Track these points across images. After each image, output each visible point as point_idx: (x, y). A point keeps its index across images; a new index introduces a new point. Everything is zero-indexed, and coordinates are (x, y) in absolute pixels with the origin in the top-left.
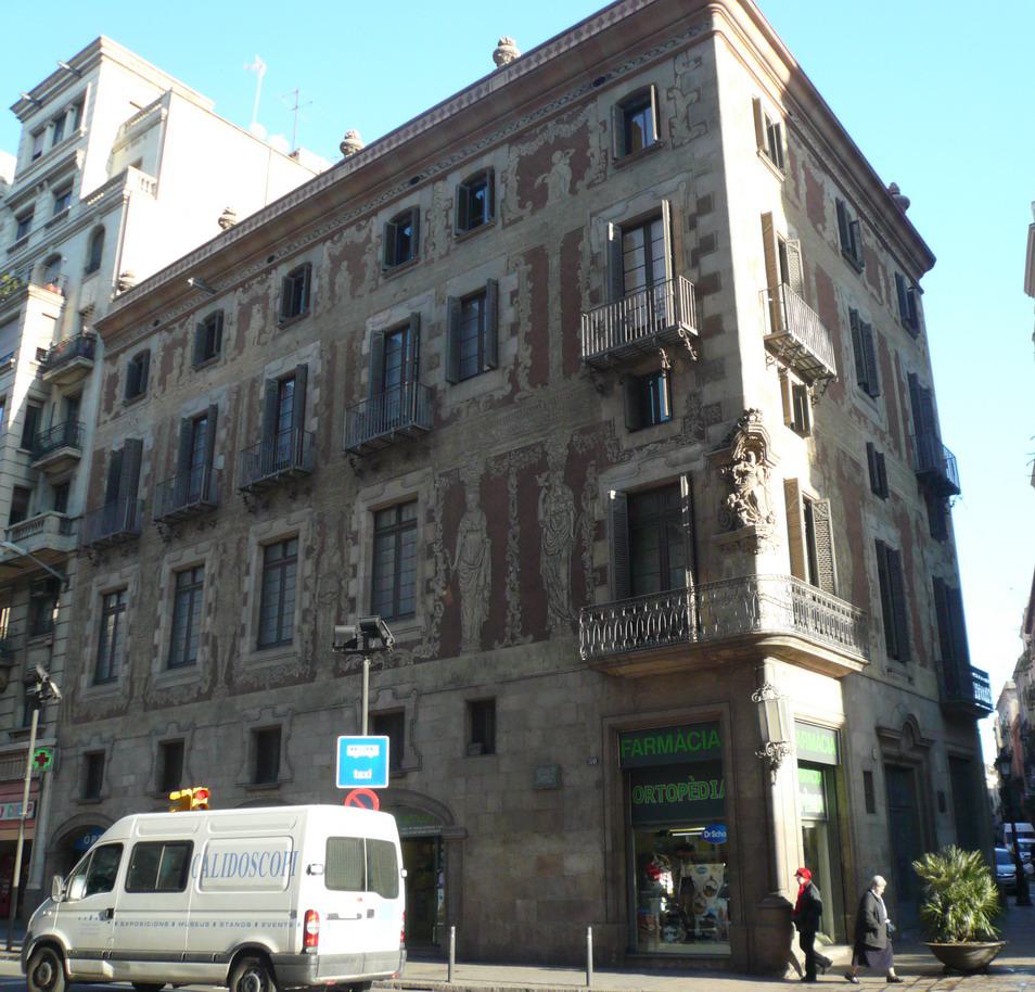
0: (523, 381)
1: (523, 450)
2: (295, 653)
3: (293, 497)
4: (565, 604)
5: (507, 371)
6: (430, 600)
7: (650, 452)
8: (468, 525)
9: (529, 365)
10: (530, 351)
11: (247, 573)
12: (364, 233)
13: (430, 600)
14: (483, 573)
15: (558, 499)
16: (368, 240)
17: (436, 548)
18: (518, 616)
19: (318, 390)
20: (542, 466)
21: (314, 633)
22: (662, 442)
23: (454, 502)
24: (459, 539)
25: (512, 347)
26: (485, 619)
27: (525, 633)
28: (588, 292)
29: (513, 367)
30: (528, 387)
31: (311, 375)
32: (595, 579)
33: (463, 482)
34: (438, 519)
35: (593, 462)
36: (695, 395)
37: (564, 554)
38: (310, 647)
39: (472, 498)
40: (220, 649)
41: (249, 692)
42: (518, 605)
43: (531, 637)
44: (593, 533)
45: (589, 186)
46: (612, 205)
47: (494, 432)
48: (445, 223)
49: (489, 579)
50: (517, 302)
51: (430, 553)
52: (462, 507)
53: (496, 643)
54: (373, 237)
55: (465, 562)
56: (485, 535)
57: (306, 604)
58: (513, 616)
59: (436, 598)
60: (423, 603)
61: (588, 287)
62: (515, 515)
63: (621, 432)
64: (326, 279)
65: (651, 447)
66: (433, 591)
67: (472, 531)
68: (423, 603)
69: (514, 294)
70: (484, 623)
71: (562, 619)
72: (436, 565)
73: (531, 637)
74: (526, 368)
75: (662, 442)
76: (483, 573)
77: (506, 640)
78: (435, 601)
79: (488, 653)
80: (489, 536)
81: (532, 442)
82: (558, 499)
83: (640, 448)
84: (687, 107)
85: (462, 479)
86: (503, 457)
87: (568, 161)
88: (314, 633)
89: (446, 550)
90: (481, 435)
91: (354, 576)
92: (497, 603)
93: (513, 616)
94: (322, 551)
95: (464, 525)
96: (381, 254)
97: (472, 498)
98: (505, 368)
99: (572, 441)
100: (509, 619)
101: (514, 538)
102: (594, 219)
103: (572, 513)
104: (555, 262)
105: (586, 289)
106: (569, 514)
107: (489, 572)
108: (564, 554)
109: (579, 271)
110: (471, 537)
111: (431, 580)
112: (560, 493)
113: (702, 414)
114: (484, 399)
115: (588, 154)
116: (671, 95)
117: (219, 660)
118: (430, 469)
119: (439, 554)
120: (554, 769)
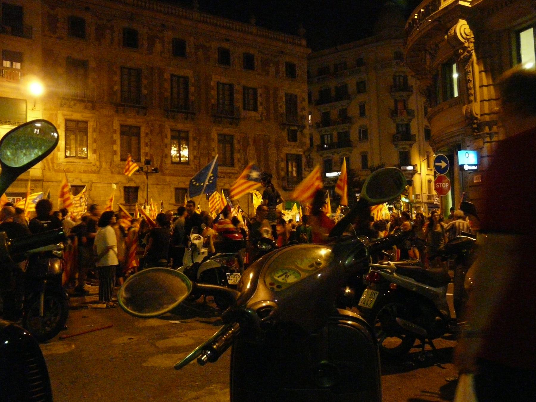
2: (192, 168)
3: (186, 119)
6: (240, 164)
17: (241, 151)
19: (193, 88)
20: (269, 141)
24: (248, 151)
25: (260, 108)
38: (198, 167)
39: (251, 142)
51: (239, 152)
57: (195, 154)
91: (214, 150)
97: (251, 142)
110: (251, 151)
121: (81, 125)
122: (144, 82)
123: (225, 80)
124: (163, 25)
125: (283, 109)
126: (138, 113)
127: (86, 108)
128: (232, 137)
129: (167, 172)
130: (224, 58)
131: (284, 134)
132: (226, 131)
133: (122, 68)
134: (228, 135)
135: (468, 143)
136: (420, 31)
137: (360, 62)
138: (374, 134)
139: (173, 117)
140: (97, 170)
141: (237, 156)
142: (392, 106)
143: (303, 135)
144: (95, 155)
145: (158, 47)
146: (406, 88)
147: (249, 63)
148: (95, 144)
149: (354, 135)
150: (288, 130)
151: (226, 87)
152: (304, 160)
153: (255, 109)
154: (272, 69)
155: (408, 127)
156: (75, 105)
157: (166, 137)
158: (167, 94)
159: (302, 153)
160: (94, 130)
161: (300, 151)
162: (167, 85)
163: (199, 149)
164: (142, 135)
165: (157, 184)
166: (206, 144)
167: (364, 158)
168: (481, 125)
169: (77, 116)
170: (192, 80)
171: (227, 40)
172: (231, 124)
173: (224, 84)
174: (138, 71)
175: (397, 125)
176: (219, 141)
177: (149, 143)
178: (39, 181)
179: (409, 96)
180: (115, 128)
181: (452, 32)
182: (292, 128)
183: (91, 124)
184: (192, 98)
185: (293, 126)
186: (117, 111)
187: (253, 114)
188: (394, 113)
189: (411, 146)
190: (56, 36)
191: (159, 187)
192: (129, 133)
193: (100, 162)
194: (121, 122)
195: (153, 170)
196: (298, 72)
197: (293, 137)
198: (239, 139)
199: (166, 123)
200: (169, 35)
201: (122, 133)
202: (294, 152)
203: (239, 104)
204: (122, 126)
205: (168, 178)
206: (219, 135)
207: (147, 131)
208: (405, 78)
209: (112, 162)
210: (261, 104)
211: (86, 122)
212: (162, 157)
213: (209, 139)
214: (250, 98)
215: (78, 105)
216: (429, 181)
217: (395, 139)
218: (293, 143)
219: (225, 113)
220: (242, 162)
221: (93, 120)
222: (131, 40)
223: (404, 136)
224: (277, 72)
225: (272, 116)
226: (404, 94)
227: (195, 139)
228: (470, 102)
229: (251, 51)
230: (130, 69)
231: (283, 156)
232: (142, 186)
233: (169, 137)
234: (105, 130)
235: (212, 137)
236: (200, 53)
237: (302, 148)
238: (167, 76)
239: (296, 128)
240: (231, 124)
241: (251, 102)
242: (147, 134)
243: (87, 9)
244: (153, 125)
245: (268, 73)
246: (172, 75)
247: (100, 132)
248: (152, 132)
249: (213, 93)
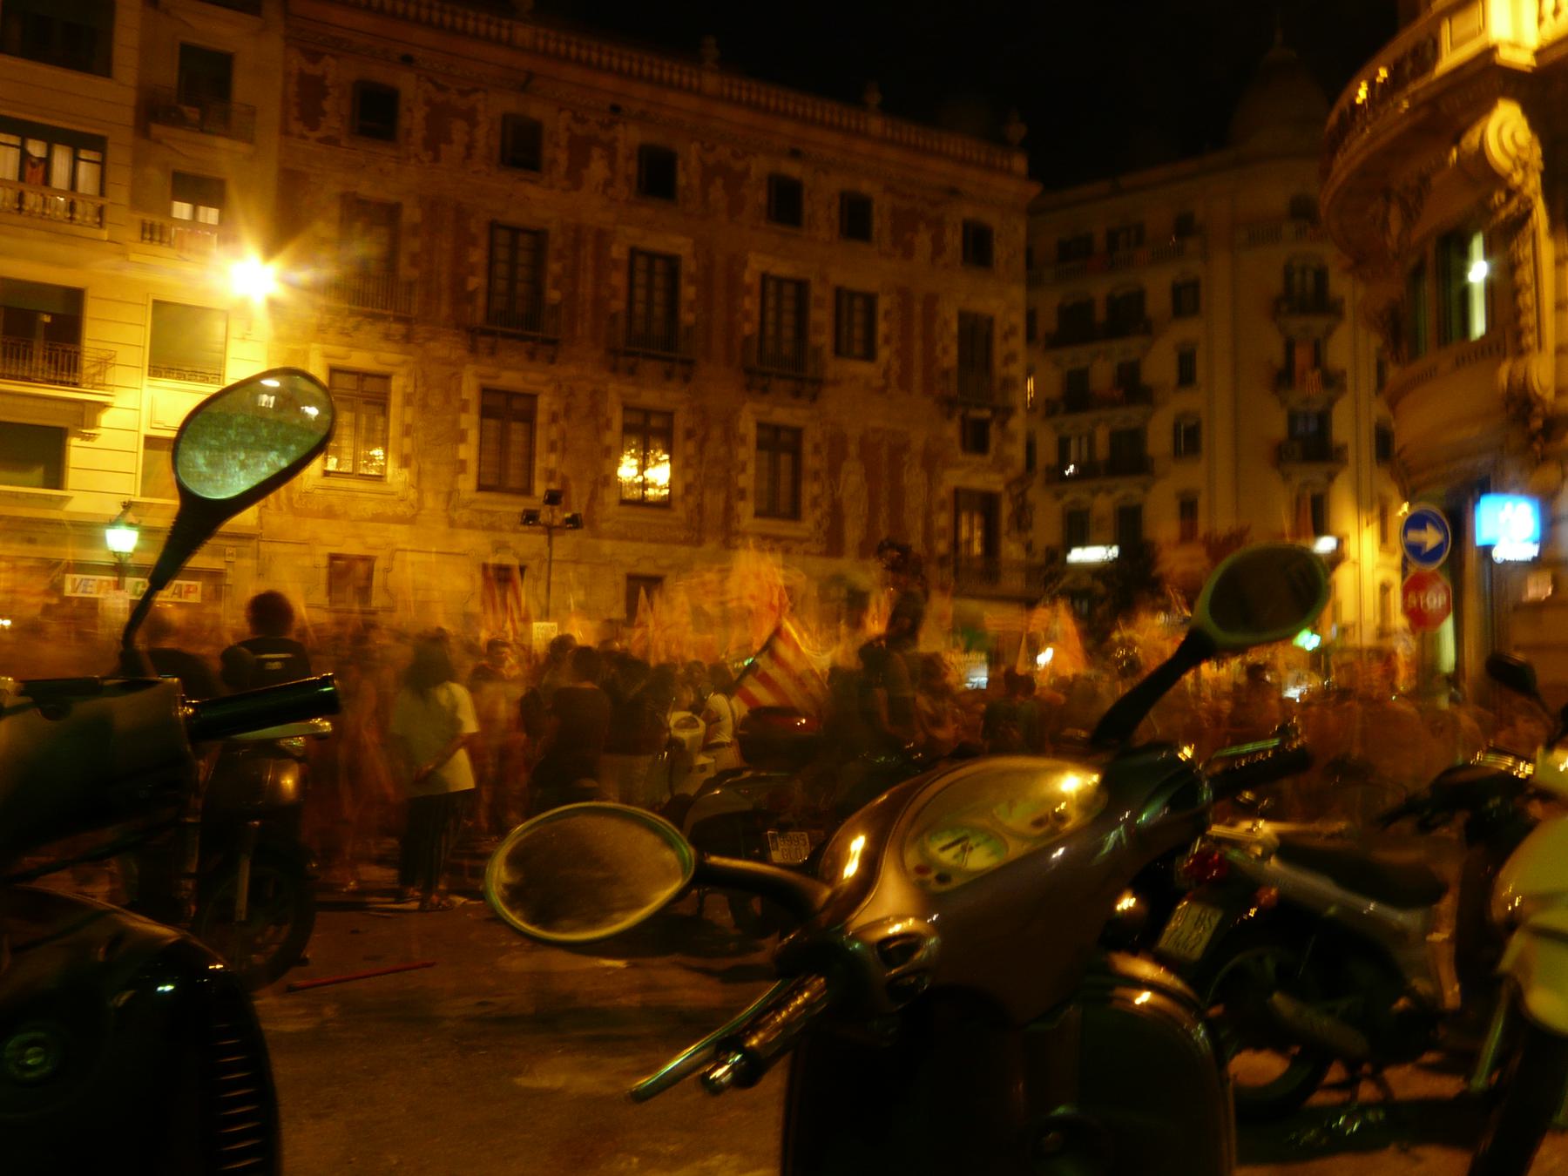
3: (669, 376)
21: (700, 507)
23: (836, 447)
24: (843, 476)
25: (884, 353)
39: (853, 449)
51: (816, 476)
69: (887, 313)
88: (700, 507)
91: (743, 470)
94: (705, 439)
97: (853, 449)
104: (918, 308)
121: (371, 385)
122: (554, 267)
123: (783, 269)
124: (615, 109)
125: (949, 358)
126: (532, 356)
127: (387, 337)
128: (797, 433)
129: (605, 526)
130: (786, 203)
131: (952, 430)
132: (782, 415)
133: (494, 226)
134: (787, 428)
135: (1512, 475)
136: (1372, 139)
137: (1185, 227)
138: (1218, 437)
139: (632, 371)
140: (410, 512)
141: (810, 489)
142: (1279, 359)
143: (1009, 437)
144: (405, 472)
145: (597, 169)
146: (1320, 303)
147: (855, 219)
148: (407, 441)
149: (1159, 439)
150: (963, 418)
151: (789, 290)
152: (1006, 509)
153: (869, 355)
154: (923, 240)
155: (1324, 420)
156: (356, 328)
157: (608, 425)
158: (618, 305)
159: (1000, 488)
160: (408, 400)
162: (618, 279)
163: (701, 462)
164: (541, 418)
165: (577, 562)
166: (722, 451)
167: (1188, 508)
168: (1553, 426)
169: (360, 360)
170: (689, 266)
171: (795, 154)
173: (780, 281)
174: (539, 237)
175: (1292, 419)
176: (761, 445)
177: (559, 445)
178: (249, 537)
179: (1329, 332)
180: (465, 396)
181: (1471, 140)
182: (975, 414)
183: (398, 385)
184: (687, 317)
185: (979, 407)
186: (473, 350)
187: (863, 369)
188: (1284, 378)
189: (1331, 478)
190: (318, 134)
191: (583, 569)
192: (504, 411)
193: (421, 492)
194: (487, 382)
195: (568, 521)
196: (1000, 251)
197: (976, 439)
199: (611, 386)
200: (630, 136)
201: (485, 412)
203: (823, 339)
204: (485, 391)
205: (607, 546)
206: (760, 426)
207: (555, 407)
208: (1321, 276)
209: (451, 494)
211: (386, 377)
212: (595, 483)
213: (731, 437)
214: (856, 321)
215: (368, 328)
216: (1385, 588)
217: (1281, 456)
218: (976, 459)
219: (783, 364)
220: (825, 505)
221: (403, 370)
222: (522, 150)
223: (1311, 447)
224: (938, 249)
225: (917, 377)
226: (1319, 323)
227: (689, 435)
228: (1521, 352)
229: (866, 187)
230: (515, 231)
231: (943, 492)
232: (534, 564)
233: (617, 424)
234: (436, 401)
235: (742, 430)
236: (717, 192)
237: (1002, 470)
238: (618, 252)
239: (987, 414)
240: (797, 394)
241: (858, 333)
242: (554, 418)
243: (407, 60)
244: (572, 393)
245: (908, 253)
246: (634, 252)
247: (424, 406)
248: (568, 410)
249: (750, 304)
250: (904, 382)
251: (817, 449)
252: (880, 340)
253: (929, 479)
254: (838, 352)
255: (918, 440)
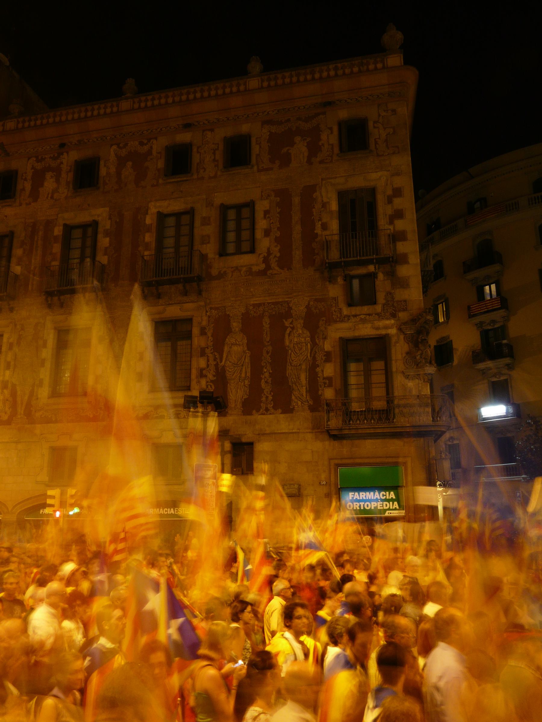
0: (274, 265)
1: (273, 303)
4: (305, 396)
5: (261, 256)
6: (203, 382)
7: (361, 319)
8: (233, 341)
9: (278, 255)
10: (279, 247)
11: (45, 345)
12: (146, 148)
13: (203, 382)
14: (244, 370)
15: (299, 335)
16: (150, 152)
17: (208, 351)
18: (270, 398)
19: (107, 239)
20: (288, 314)
22: (369, 315)
23: (221, 328)
24: (226, 349)
25: (264, 244)
26: (246, 397)
27: (275, 408)
28: (320, 222)
29: (266, 255)
30: (277, 268)
31: (100, 229)
32: (325, 383)
33: (229, 315)
34: (209, 334)
35: (324, 318)
36: (391, 293)
37: (304, 367)
39: (236, 325)
40: (19, 393)
41: (48, 422)
42: (271, 391)
43: (280, 411)
44: (324, 358)
45: (321, 162)
46: (336, 178)
47: (252, 290)
48: (213, 158)
49: (249, 374)
50: (269, 217)
51: (203, 353)
52: (228, 330)
53: (254, 411)
54: (154, 153)
55: (230, 362)
56: (246, 349)
58: (267, 397)
59: (208, 380)
60: (199, 382)
61: (320, 220)
62: (268, 339)
63: (342, 305)
64: (113, 170)
65: (363, 317)
66: (206, 376)
67: (236, 344)
68: (199, 382)
69: (266, 212)
70: (245, 399)
71: (302, 403)
72: (208, 361)
73: (280, 411)
74: (275, 256)
75: (369, 315)
76: (244, 370)
77: (262, 410)
78: (207, 382)
79: (249, 417)
80: (248, 349)
81: (280, 300)
82: (299, 335)
83: (355, 316)
84: (387, 135)
85: (228, 313)
86: (259, 305)
87: (306, 144)
89: (216, 354)
90: (242, 290)
92: (255, 389)
93: (267, 397)
95: (229, 340)
96: (161, 164)
97: (236, 325)
98: (260, 254)
99: (309, 304)
100: (264, 399)
101: (268, 353)
102: (324, 182)
103: (309, 345)
104: (296, 200)
105: (319, 220)
106: (307, 345)
107: (249, 370)
108: (304, 367)
109: (314, 209)
110: (235, 348)
111: (204, 369)
112: (301, 332)
113: (395, 304)
114: (244, 269)
115: (320, 143)
116: (376, 125)
117: (19, 399)
118: (202, 303)
119: (210, 355)
120: (296, 486)
129: (38, 415)
131: (335, 291)
147: (237, 153)
150: (349, 279)
152: (399, 350)
159: (393, 331)
161: (386, 327)
171: (187, 126)
172: (185, 293)
187: (245, 260)
198: (204, 323)
200: (71, 157)
202: (366, 330)
210: (267, 233)
218: (366, 309)
220: (210, 377)
225: (297, 254)
237: (393, 316)
239: (371, 268)
245: (286, 160)
250: (285, 262)
251: (203, 332)
252: (259, 234)
253: (313, 338)
254: (222, 253)
255: (299, 307)
